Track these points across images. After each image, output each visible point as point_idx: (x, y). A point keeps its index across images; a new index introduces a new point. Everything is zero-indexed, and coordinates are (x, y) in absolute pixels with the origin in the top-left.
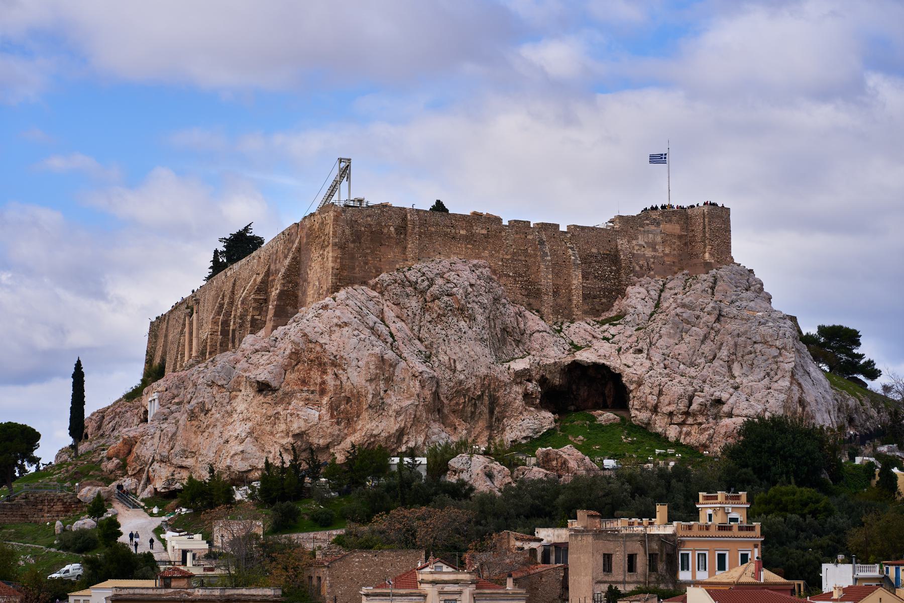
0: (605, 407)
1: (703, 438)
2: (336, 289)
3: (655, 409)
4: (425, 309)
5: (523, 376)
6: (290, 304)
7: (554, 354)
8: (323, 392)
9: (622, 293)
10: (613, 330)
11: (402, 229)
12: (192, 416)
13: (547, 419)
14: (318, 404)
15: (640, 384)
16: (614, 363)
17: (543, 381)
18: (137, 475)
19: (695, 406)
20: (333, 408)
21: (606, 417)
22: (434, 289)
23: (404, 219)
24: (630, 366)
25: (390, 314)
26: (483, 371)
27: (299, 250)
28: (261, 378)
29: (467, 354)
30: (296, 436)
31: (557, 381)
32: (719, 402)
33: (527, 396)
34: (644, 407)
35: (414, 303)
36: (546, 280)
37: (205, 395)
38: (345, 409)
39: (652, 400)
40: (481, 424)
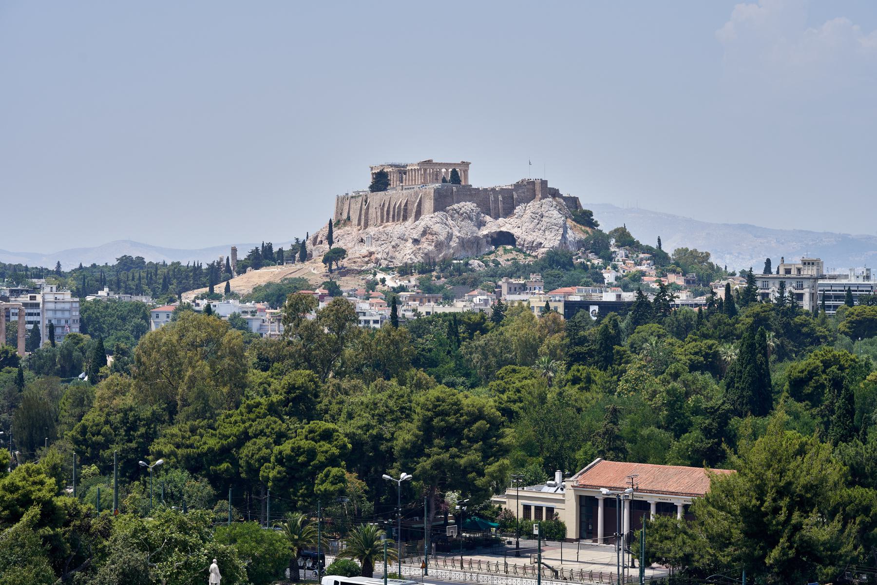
0: (509, 244)
2: (434, 212)
3: (523, 245)
5: (487, 236)
6: (418, 214)
12: (393, 247)
16: (512, 231)
17: (492, 237)
18: (376, 263)
21: (509, 247)
24: (516, 232)
28: (416, 237)
31: (495, 236)
32: (541, 244)
33: (487, 242)
34: (520, 245)
36: (492, 206)
37: (398, 241)
40: (475, 250)
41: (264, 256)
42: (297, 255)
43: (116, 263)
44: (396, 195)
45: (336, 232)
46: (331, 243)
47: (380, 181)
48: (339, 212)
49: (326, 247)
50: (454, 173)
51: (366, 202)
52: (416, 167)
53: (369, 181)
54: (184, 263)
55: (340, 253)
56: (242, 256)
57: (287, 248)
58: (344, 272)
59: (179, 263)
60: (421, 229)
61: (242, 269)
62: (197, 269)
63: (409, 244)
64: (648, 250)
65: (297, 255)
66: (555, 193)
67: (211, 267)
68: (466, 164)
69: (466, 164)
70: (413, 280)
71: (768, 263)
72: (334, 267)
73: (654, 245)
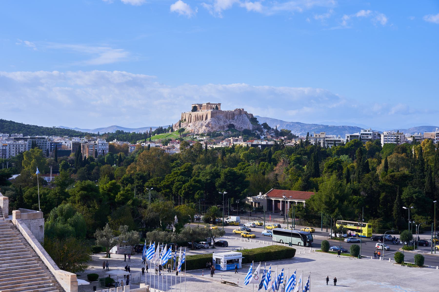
7: (229, 123)
13: (228, 129)
21: (233, 128)
24: (235, 124)
29: (222, 123)
36: (228, 116)
41: (160, 131)
42: (170, 130)
43: (115, 132)
44: (200, 113)
45: (182, 124)
47: (195, 109)
48: (182, 118)
49: (179, 128)
50: (217, 107)
53: (191, 109)
54: (136, 133)
55: (183, 130)
56: (153, 130)
57: (167, 128)
58: (185, 135)
59: (135, 133)
60: (207, 123)
61: (154, 134)
62: (140, 134)
63: (204, 127)
64: (273, 129)
65: (170, 130)
66: (246, 113)
67: (145, 133)
68: (220, 104)
69: (220, 104)
70: (205, 138)
71: (308, 133)
72: (181, 134)
73: (275, 128)
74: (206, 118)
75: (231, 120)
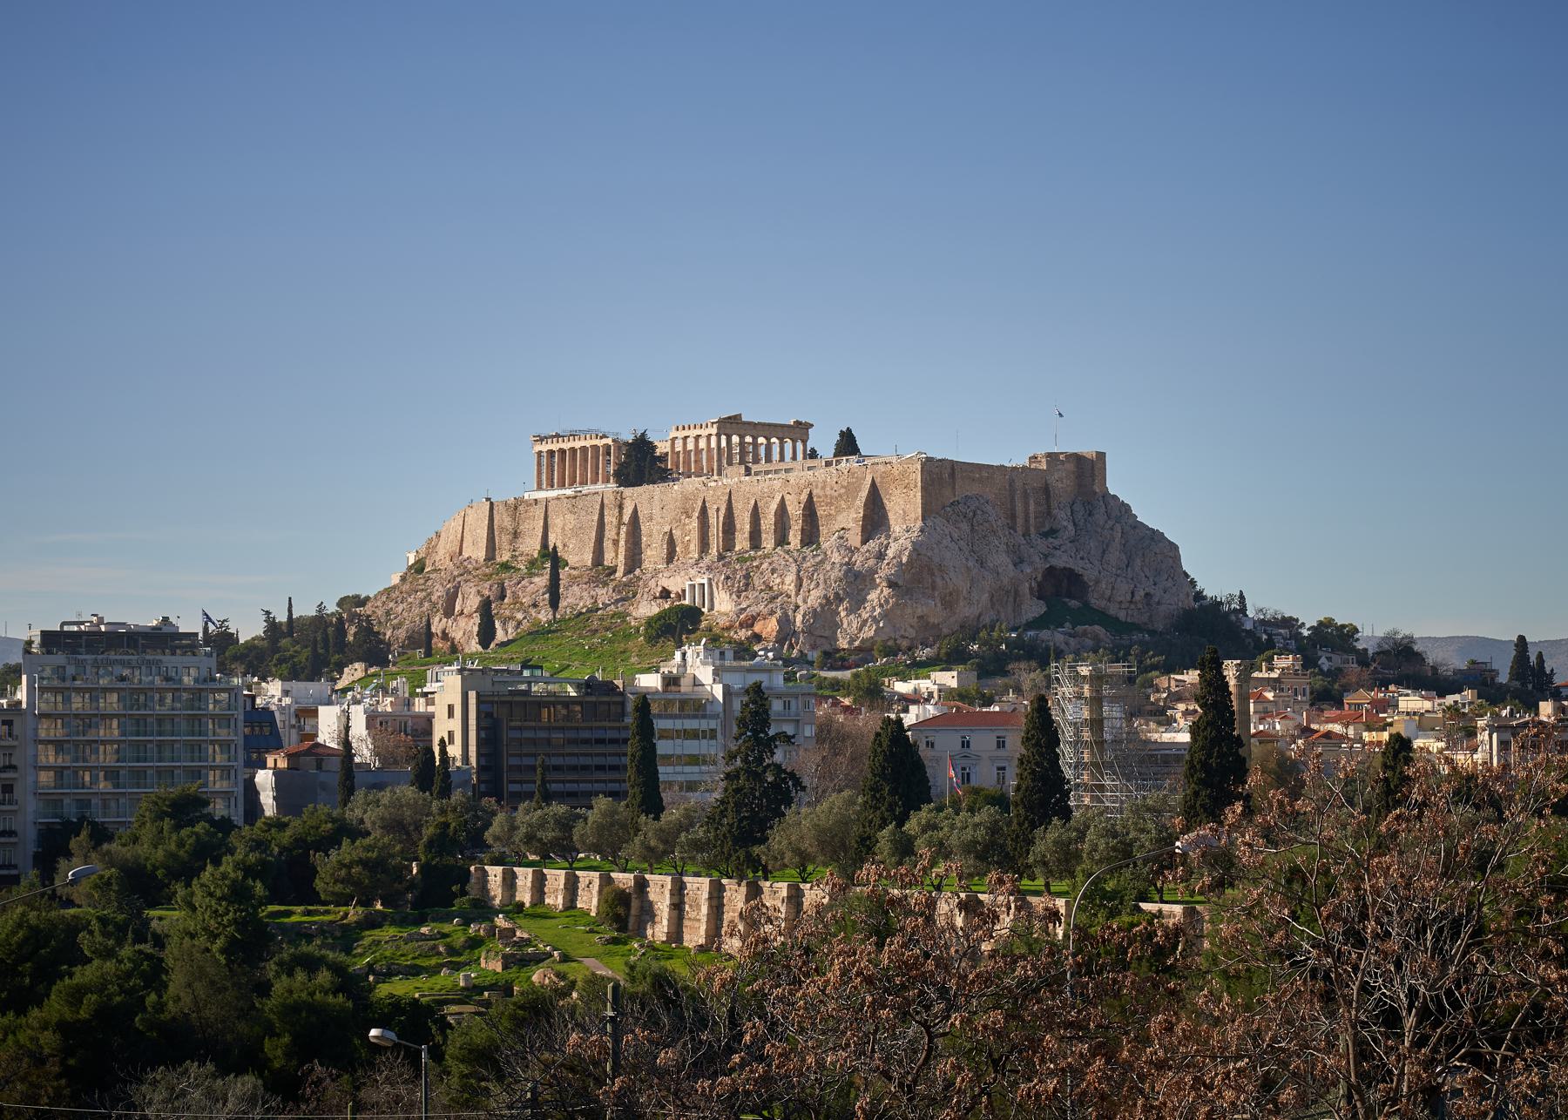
1: (1145, 618)
4: (972, 530)
8: (934, 588)
9: (1049, 513)
10: (1057, 543)
11: (952, 475)
14: (933, 597)
15: (1097, 582)
19: (1137, 598)
20: (942, 599)
22: (979, 517)
23: (953, 469)
25: (956, 536)
26: (1012, 574)
27: (873, 483)
30: (920, 618)
35: (965, 526)
36: (1019, 507)
38: (949, 603)
39: (1108, 593)
40: (1010, 609)
46: (554, 603)
51: (621, 507)
52: (704, 432)
74: (875, 519)
75: (1042, 544)
